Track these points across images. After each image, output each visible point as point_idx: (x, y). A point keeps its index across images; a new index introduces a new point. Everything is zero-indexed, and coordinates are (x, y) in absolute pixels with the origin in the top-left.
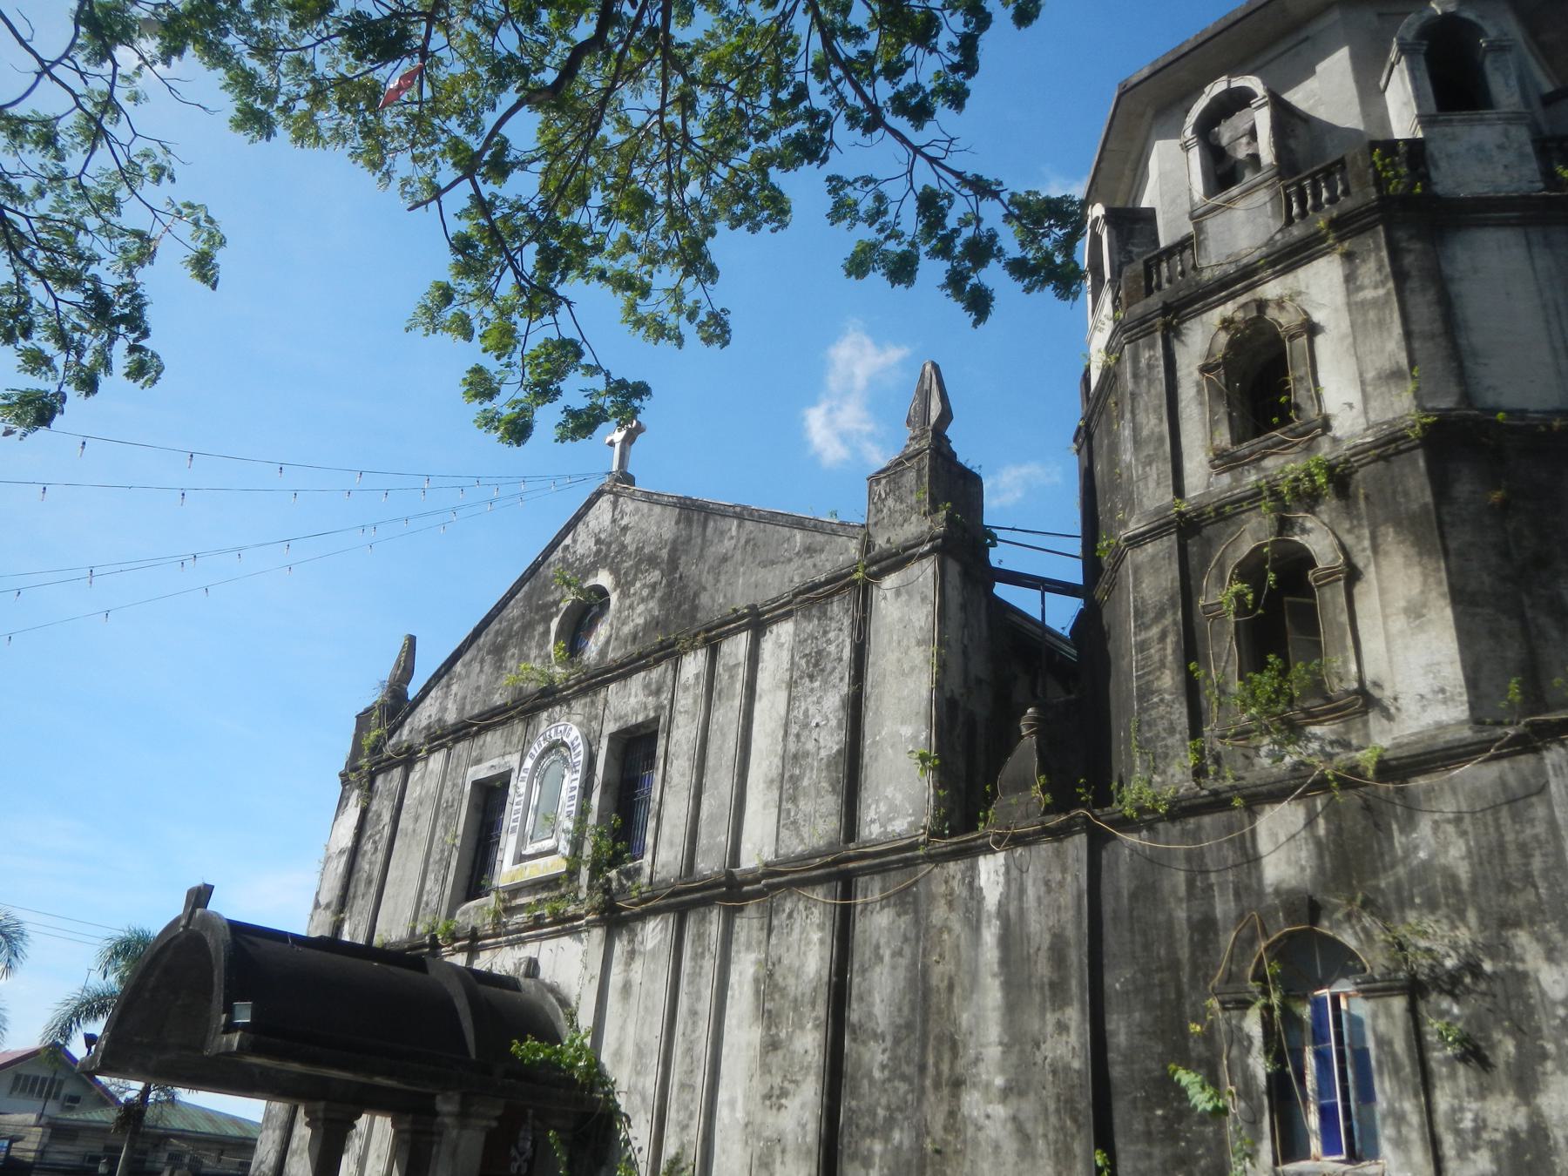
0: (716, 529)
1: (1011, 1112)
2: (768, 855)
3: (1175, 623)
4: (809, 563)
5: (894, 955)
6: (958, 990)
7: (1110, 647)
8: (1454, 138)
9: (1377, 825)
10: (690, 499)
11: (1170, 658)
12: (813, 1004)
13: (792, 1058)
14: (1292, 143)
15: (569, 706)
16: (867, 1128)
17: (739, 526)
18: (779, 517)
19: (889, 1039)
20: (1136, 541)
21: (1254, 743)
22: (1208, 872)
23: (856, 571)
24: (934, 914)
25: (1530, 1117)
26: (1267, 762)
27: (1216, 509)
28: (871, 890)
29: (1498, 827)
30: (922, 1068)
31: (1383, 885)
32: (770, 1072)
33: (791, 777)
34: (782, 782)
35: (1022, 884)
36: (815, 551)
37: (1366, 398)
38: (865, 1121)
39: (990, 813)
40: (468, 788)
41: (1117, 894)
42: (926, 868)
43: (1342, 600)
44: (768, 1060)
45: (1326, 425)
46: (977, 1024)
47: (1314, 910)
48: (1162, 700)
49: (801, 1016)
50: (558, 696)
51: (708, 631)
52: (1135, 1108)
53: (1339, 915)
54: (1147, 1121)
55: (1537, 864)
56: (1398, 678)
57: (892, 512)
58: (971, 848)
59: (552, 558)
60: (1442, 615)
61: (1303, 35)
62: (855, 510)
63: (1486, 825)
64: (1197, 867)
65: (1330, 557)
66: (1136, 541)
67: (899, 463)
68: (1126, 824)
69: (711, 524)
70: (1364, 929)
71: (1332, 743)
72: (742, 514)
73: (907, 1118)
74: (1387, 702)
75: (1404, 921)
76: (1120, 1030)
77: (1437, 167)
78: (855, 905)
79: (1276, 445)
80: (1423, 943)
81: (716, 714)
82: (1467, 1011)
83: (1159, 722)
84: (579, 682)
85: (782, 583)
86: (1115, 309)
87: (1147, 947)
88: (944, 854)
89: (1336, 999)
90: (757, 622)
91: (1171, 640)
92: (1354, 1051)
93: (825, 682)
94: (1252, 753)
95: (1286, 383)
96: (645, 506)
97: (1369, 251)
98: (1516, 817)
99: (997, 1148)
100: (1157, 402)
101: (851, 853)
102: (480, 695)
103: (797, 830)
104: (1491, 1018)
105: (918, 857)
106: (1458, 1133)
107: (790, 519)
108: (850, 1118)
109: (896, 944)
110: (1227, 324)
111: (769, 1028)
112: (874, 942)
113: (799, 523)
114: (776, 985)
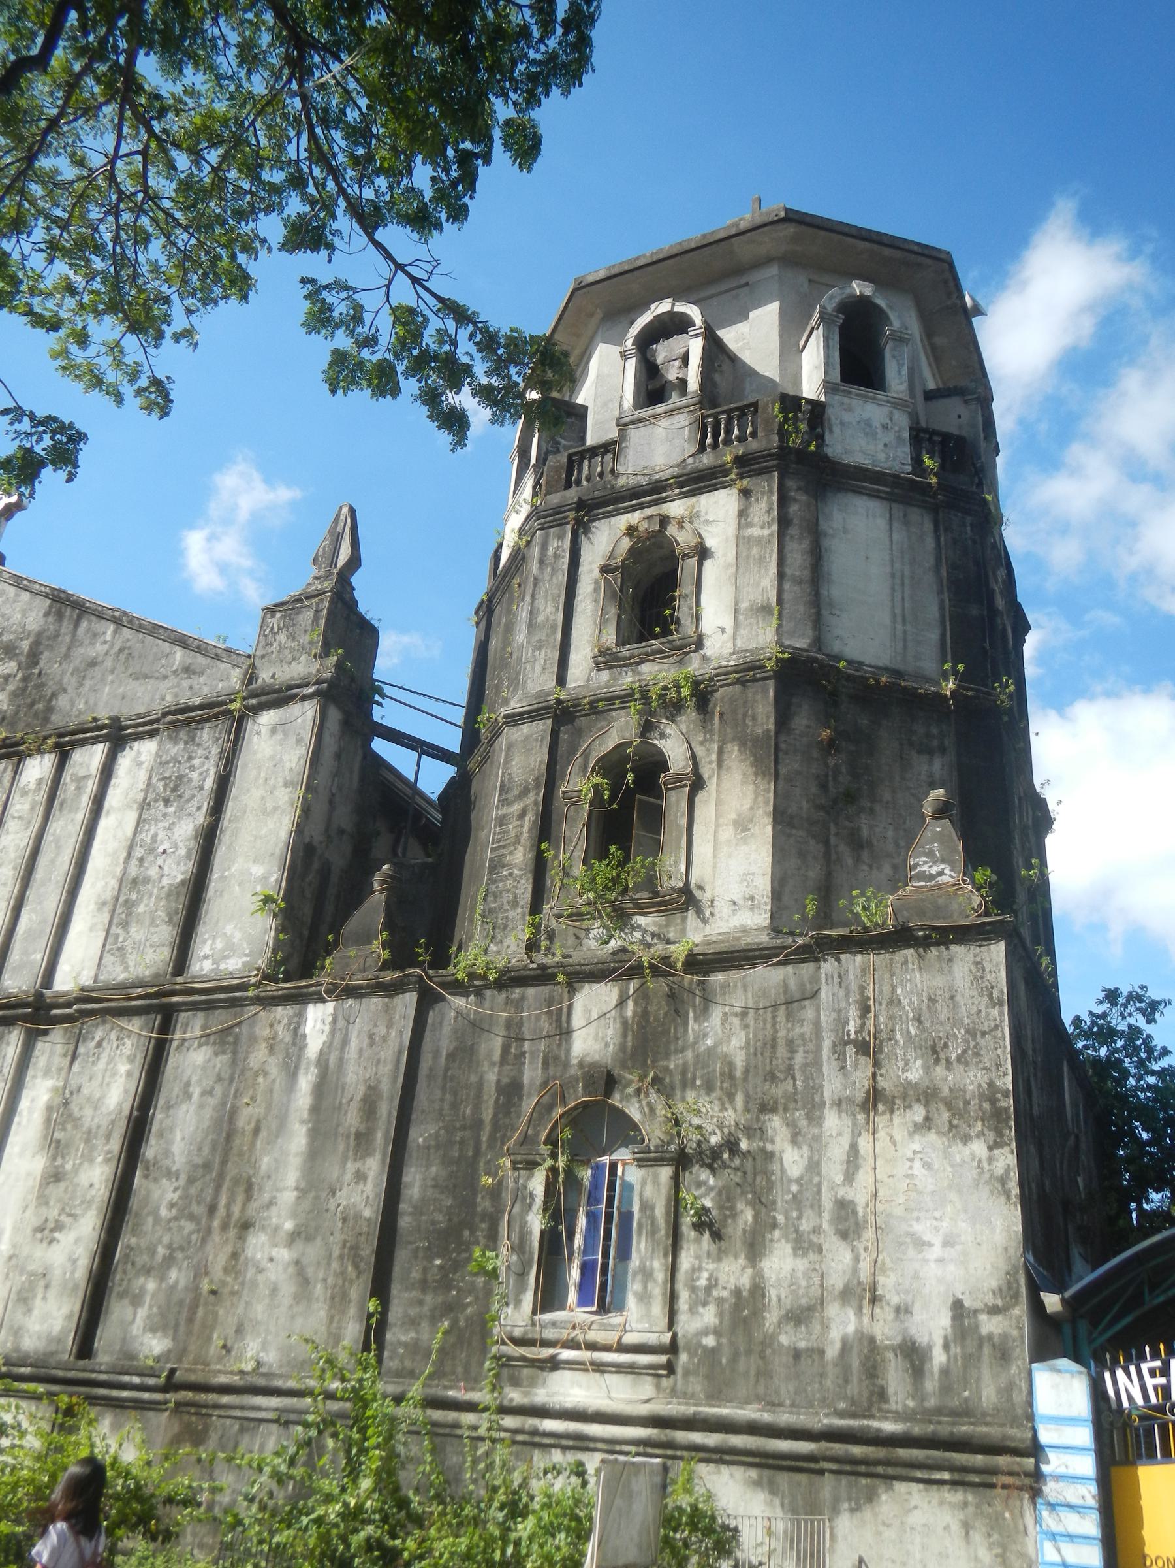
0: (88, 630)
1: (295, 1255)
2: (87, 980)
3: (536, 803)
4: (185, 684)
5: (203, 1094)
6: (263, 1134)
7: (473, 816)
8: (849, 409)
9: (677, 1011)
11: (525, 835)
12: (108, 1137)
14: (717, 377)
17: (115, 632)
19: (182, 1181)
20: (514, 720)
21: (586, 924)
22: (524, 1040)
23: (233, 701)
24: (252, 1056)
25: (753, 1278)
26: (593, 944)
27: (591, 703)
28: (191, 1026)
29: (774, 1024)
30: (212, 1209)
31: (672, 1066)
32: (47, 1204)
33: (126, 901)
34: (115, 906)
35: (346, 1034)
36: (194, 673)
37: (736, 624)
38: (142, 1259)
39: (327, 962)
41: (436, 1053)
42: (253, 1009)
43: (684, 805)
44: (47, 1192)
45: (699, 644)
46: (277, 1169)
47: (610, 1082)
48: (511, 874)
49: (92, 1149)
51: (60, 736)
52: (416, 1257)
53: (630, 1090)
54: (425, 1270)
55: (799, 1058)
56: (719, 882)
57: (282, 648)
58: (301, 995)
60: (764, 830)
61: (743, 280)
62: (245, 639)
63: (765, 1021)
64: (514, 1034)
65: (682, 764)
66: (514, 720)
67: (298, 600)
68: (457, 987)
69: (84, 624)
70: (649, 1104)
71: (653, 935)
72: (121, 620)
73: (187, 1258)
74: (705, 903)
75: (683, 1099)
76: (415, 1182)
77: (831, 431)
79: (654, 653)
80: (696, 1121)
81: (55, 825)
82: (720, 1184)
83: (505, 894)
85: (152, 700)
86: (535, 494)
87: (455, 1106)
88: (273, 998)
89: (613, 1166)
91: (529, 818)
92: (620, 1213)
93: (181, 808)
94: (582, 934)
95: (673, 598)
96: (11, 591)
97: (763, 493)
98: (789, 1016)
99: (274, 1290)
100: (556, 591)
101: (178, 987)
103: (123, 956)
104: (739, 1190)
105: (246, 999)
106: (693, 1289)
107: (173, 635)
108: (127, 1256)
109: (208, 1083)
110: (631, 531)
111: (54, 1158)
112: (185, 1079)
113: (182, 641)
114: (70, 1115)
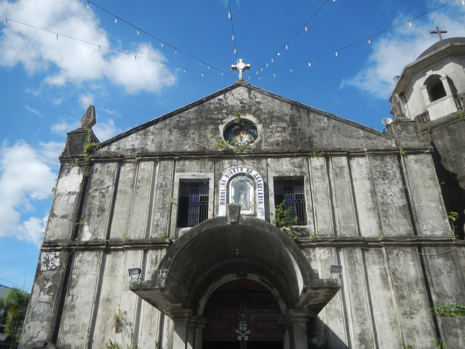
4: (369, 142)
5: (448, 272)
13: (412, 302)
15: (242, 161)
16: (453, 325)
17: (328, 120)
18: (351, 123)
19: (454, 299)
32: (403, 306)
36: (371, 139)
40: (177, 181)
42: (455, 248)
49: (413, 288)
50: (236, 156)
51: (325, 152)
59: (212, 101)
69: (312, 116)
78: (426, 255)
84: (249, 153)
88: (461, 244)
90: (350, 155)
93: (390, 182)
96: (270, 99)
109: (449, 269)
112: (438, 267)
113: (363, 128)
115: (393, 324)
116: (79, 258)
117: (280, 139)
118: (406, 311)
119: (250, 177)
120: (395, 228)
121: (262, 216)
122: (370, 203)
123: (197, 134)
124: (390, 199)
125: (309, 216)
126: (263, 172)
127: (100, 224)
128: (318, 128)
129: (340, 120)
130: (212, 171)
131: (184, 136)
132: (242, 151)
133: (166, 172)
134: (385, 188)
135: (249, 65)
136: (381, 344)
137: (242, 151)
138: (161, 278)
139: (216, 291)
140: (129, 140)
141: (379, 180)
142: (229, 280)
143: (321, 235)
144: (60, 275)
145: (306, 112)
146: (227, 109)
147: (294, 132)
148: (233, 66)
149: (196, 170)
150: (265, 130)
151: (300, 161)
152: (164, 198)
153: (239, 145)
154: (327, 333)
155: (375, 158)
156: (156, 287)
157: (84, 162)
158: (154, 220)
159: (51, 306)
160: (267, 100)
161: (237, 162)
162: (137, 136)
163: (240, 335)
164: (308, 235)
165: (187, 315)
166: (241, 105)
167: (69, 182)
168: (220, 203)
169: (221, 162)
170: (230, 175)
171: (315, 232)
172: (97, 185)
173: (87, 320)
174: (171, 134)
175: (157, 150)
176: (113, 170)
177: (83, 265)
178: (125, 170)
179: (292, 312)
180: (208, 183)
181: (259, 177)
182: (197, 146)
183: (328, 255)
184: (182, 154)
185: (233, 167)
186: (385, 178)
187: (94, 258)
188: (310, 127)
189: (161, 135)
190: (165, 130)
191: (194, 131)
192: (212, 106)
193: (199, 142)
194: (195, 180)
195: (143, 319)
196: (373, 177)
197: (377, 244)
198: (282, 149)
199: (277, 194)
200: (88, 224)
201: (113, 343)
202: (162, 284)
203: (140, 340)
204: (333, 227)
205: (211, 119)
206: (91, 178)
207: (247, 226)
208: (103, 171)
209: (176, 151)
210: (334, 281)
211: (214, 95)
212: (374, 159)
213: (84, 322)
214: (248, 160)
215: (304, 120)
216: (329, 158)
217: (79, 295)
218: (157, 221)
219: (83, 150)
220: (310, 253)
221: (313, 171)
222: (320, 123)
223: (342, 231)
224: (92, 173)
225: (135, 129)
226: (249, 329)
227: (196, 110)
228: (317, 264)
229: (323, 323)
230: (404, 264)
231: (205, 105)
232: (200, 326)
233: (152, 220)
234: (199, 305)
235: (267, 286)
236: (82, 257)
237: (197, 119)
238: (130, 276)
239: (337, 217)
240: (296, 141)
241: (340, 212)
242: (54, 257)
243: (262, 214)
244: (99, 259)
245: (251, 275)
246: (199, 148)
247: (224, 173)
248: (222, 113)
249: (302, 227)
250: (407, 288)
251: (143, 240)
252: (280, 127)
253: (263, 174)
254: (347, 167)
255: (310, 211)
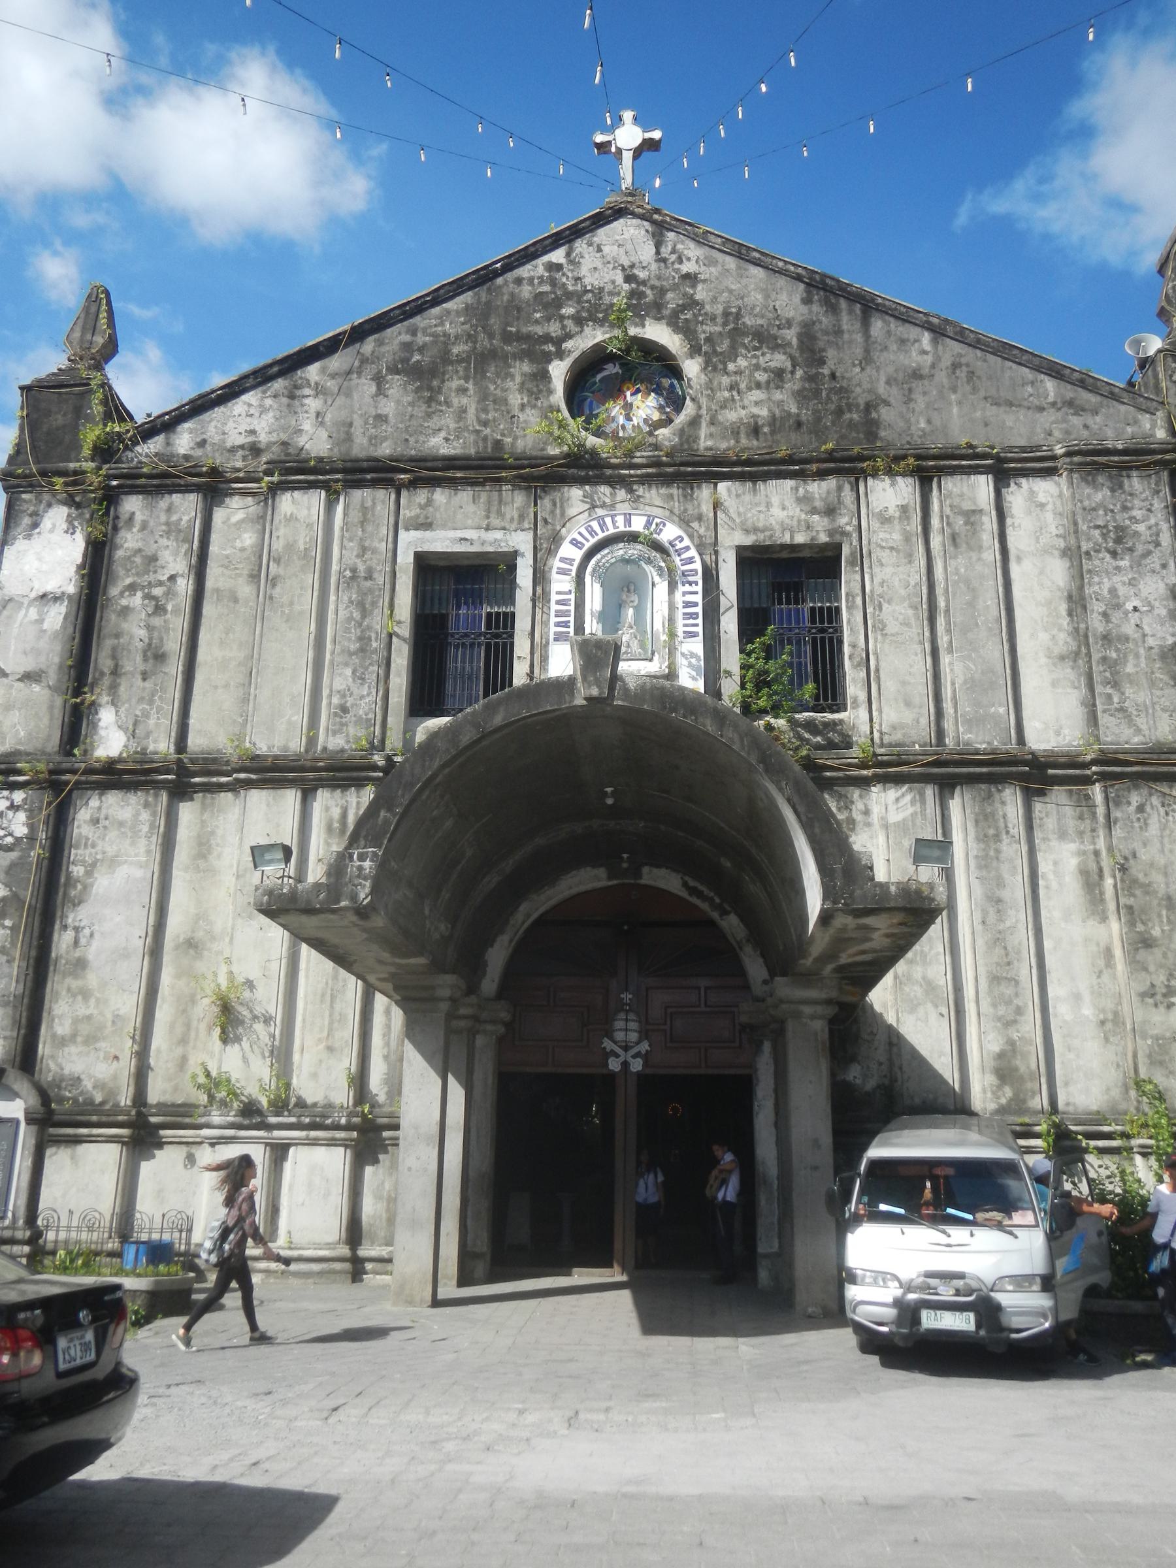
4: (1076, 421)
10: (838, 281)
15: (631, 491)
17: (935, 342)
18: (1015, 352)
32: (1146, 969)
33: (1104, 659)
36: (1083, 410)
40: (406, 560)
44: (1138, 958)
50: (609, 472)
51: (918, 457)
59: (525, 271)
69: (878, 326)
84: (657, 464)
93: (1138, 564)
96: (731, 263)
102: (386, 429)
113: (1056, 371)
114: (1135, 881)
115: (1109, 1026)
116: (90, 811)
117: (764, 412)
118: (1153, 986)
119: (657, 547)
120: (1141, 722)
121: (694, 678)
122: (1062, 636)
123: (471, 392)
124: (1133, 622)
125: (854, 680)
126: (702, 531)
127: (151, 702)
128: (896, 370)
129: (978, 343)
130: (526, 525)
131: (430, 401)
132: (630, 454)
133: (370, 528)
134: (1119, 586)
135: (657, 135)
136: (1066, 1084)
137: (630, 454)
138: (359, 876)
139: (541, 922)
140: (236, 413)
141: (1101, 555)
142: (582, 888)
143: (890, 745)
144: (31, 864)
145: (858, 312)
146: (579, 302)
147: (814, 385)
148: (599, 138)
149: (469, 522)
150: (710, 381)
151: (828, 492)
152: (364, 617)
153: (621, 434)
154: (895, 1049)
155: (1090, 478)
156: (343, 904)
157: (85, 491)
158: (331, 690)
159: (8, 961)
160: (720, 268)
161: (613, 495)
162: (262, 399)
163: (617, 1056)
164: (849, 745)
165: (446, 993)
166: (626, 287)
167: (40, 559)
168: (552, 637)
169: (557, 495)
170: (587, 540)
171: (872, 733)
172: (133, 571)
173: (128, 1004)
174: (380, 392)
175: (336, 450)
176: (185, 518)
177: (105, 835)
178: (228, 519)
179: (784, 988)
180: (512, 568)
181: (687, 548)
182: (472, 438)
183: (910, 810)
184: (419, 464)
185: (600, 512)
186: (1119, 551)
187: (138, 814)
188: (868, 369)
189: (348, 395)
190: (359, 377)
191: (462, 382)
192: (526, 292)
193: (479, 421)
194: (468, 558)
195: (306, 1004)
196: (1079, 547)
197: (1078, 772)
198: (771, 447)
199: (748, 605)
200: (113, 703)
201: (214, 1074)
202: (362, 896)
203: (300, 1067)
204: (932, 718)
205: (520, 337)
206: (114, 547)
207: (639, 711)
208: (152, 523)
209: (403, 456)
210: (924, 888)
211: (532, 249)
212: (1087, 482)
213: (118, 1009)
214: (650, 487)
215: (851, 342)
216: (931, 479)
217: (96, 927)
218: (344, 696)
219: (76, 446)
220: (852, 802)
221: (875, 524)
222: (906, 352)
223: (961, 729)
224: (116, 529)
225: (255, 373)
226: (647, 1038)
227: (467, 305)
228: (871, 837)
229: (884, 1022)
230: (1162, 837)
231: (500, 287)
232: (489, 1027)
233: (325, 692)
234: (485, 964)
235: (704, 906)
236: (99, 808)
237: (471, 338)
238: (256, 867)
239: (949, 684)
240: (818, 420)
241: (959, 668)
242: (8, 808)
243: (694, 673)
244: (154, 814)
245: (655, 870)
246: (481, 444)
247: (569, 532)
248: (562, 318)
249: (829, 716)
250: (1164, 912)
251: (299, 756)
252: (765, 370)
253: (700, 537)
254: (994, 513)
255: (859, 665)
